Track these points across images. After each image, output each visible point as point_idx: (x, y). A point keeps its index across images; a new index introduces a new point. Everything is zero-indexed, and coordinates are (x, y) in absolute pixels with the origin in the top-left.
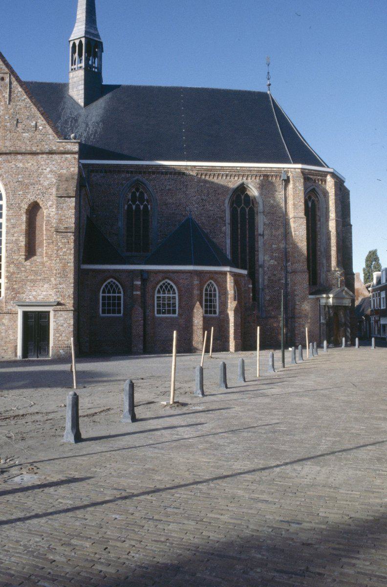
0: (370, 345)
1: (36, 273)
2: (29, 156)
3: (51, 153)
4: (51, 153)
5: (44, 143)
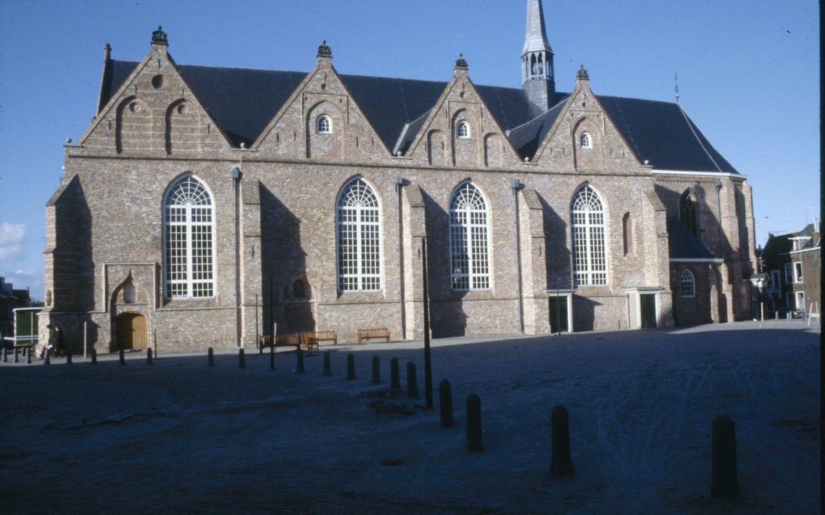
0: (774, 317)
1: (632, 266)
2: (622, 177)
3: (636, 175)
4: (636, 175)
5: (630, 167)
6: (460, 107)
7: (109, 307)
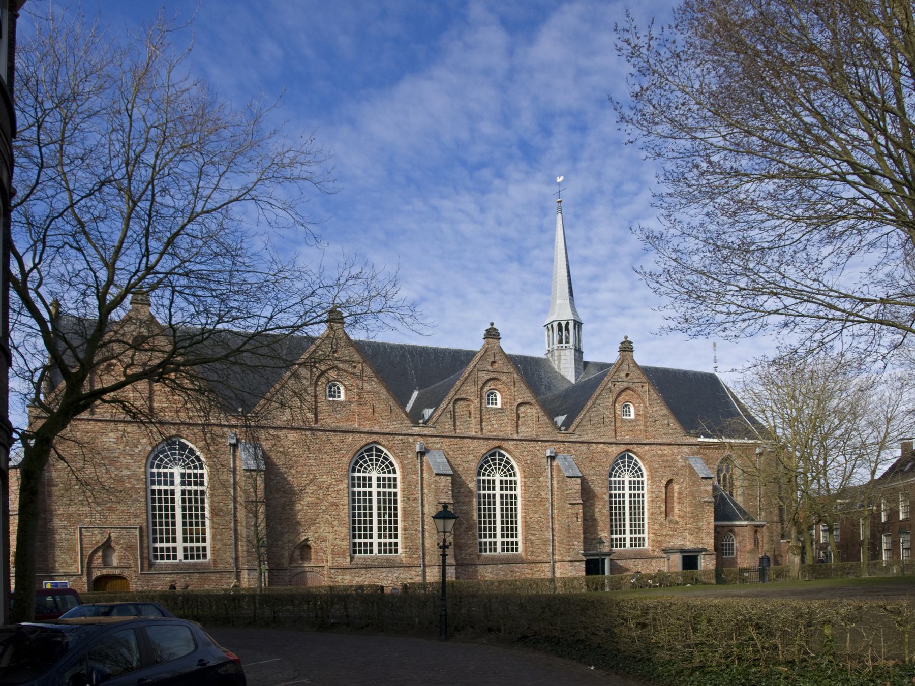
6: (489, 377)
7: (85, 569)
